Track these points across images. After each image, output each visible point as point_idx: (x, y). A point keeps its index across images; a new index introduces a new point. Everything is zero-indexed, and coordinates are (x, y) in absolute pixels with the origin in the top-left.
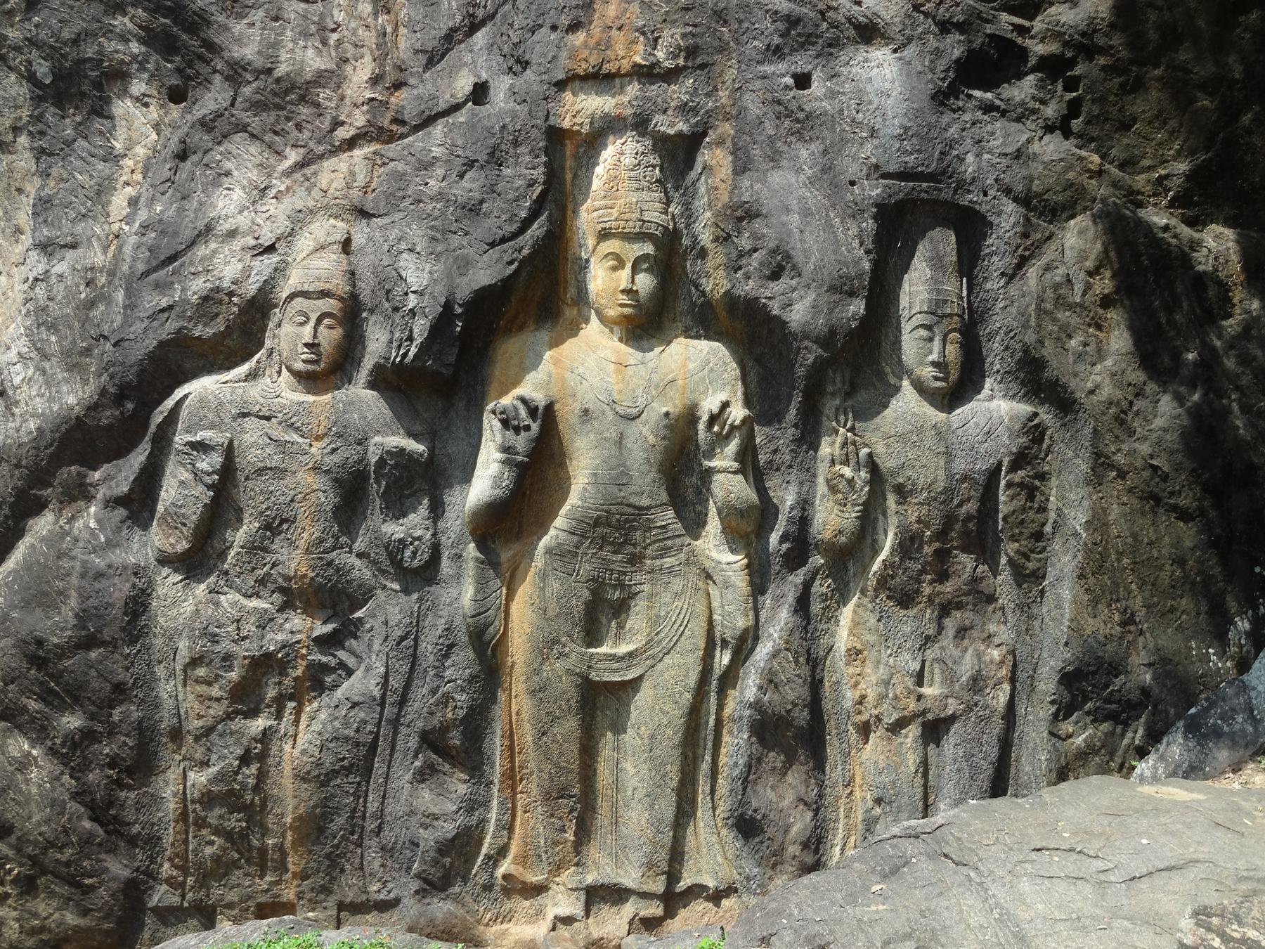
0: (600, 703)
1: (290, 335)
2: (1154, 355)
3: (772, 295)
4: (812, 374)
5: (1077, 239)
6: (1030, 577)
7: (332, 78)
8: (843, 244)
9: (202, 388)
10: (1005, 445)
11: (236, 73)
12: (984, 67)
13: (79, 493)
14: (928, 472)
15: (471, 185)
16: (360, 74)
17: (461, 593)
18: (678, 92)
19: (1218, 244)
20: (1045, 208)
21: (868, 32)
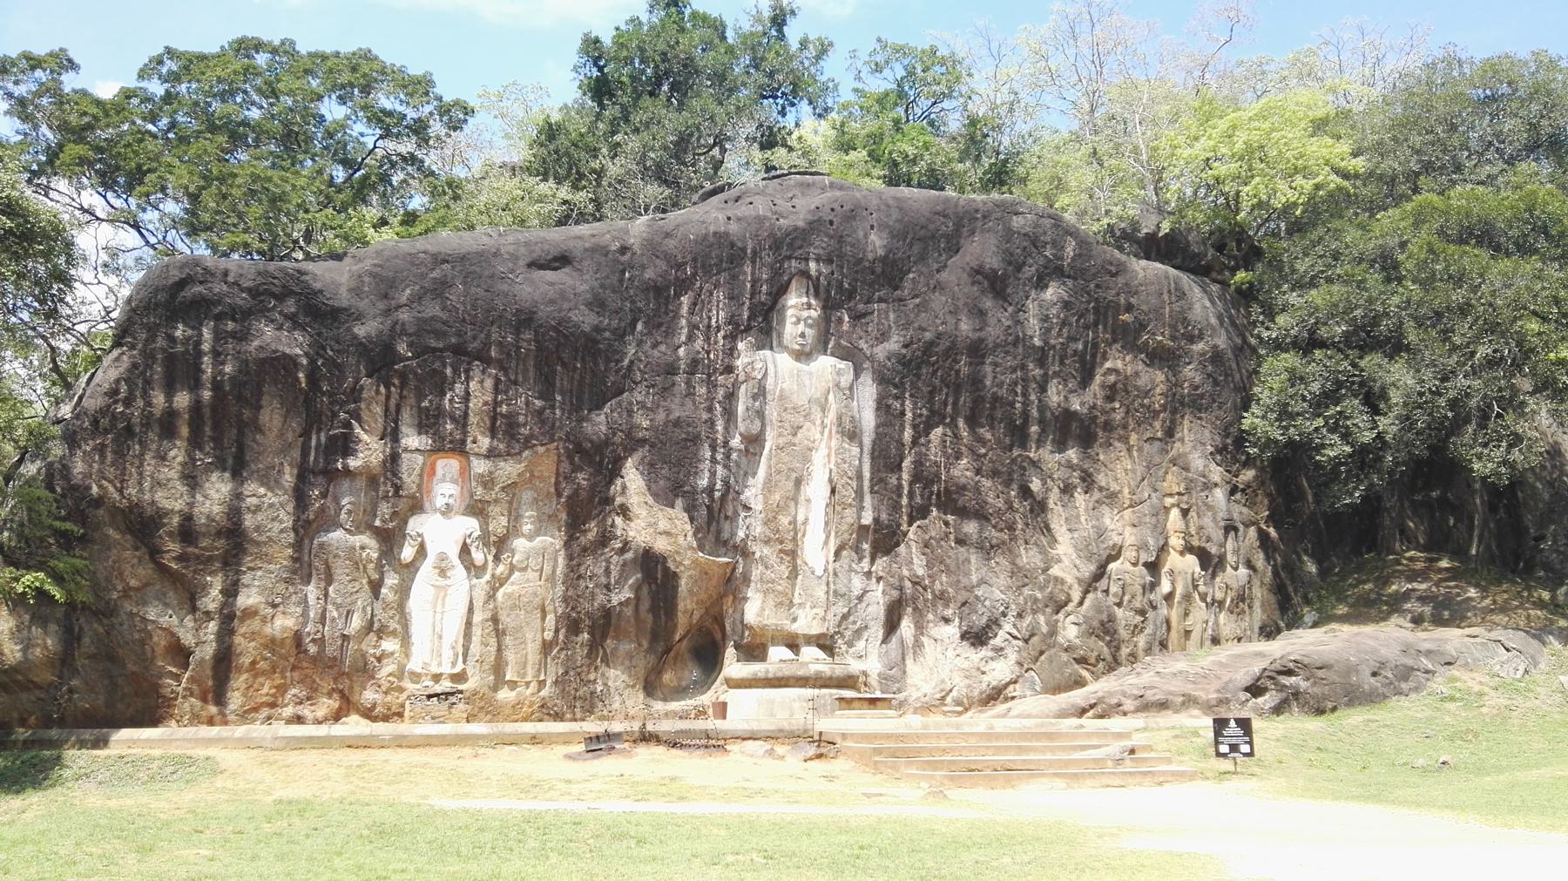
0: (1188, 633)
1: (1129, 554)
2: (1268, 558)
3: (1208, 546)
4: (1210, 563)
5: (1252, 531)
6: (1250, 607)
7: (1120, 492)
8: (1217, 535)
9: (1112, 566)
10: (1246, 579)
11: (1101, 489)
12: (1233, 492)
13: (1096, 589)
14: (1235, 585)
15: (1154, 520)
16: (1126, 491)
17: (1164, 611)
18: (1185, 498)
19: (1272, 531)
20: (1247, 526)
21: (1216, 485)
